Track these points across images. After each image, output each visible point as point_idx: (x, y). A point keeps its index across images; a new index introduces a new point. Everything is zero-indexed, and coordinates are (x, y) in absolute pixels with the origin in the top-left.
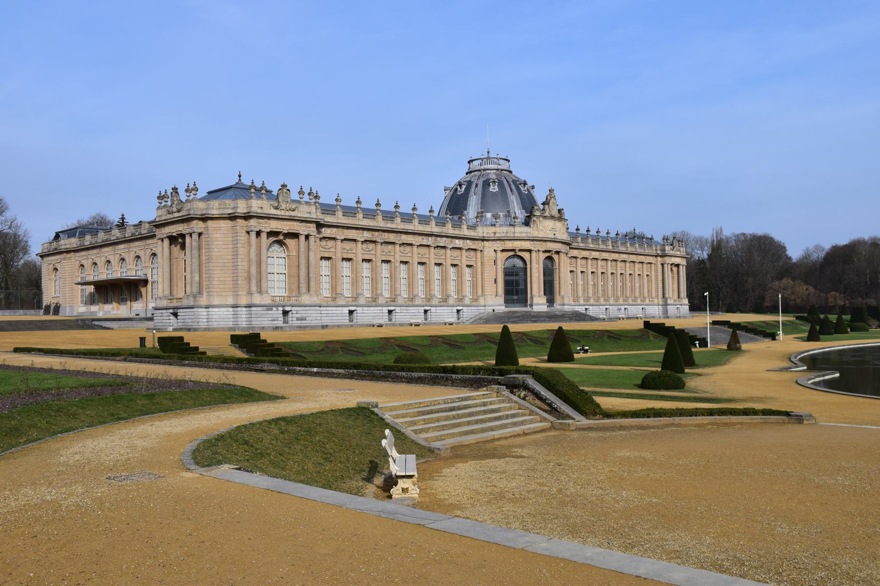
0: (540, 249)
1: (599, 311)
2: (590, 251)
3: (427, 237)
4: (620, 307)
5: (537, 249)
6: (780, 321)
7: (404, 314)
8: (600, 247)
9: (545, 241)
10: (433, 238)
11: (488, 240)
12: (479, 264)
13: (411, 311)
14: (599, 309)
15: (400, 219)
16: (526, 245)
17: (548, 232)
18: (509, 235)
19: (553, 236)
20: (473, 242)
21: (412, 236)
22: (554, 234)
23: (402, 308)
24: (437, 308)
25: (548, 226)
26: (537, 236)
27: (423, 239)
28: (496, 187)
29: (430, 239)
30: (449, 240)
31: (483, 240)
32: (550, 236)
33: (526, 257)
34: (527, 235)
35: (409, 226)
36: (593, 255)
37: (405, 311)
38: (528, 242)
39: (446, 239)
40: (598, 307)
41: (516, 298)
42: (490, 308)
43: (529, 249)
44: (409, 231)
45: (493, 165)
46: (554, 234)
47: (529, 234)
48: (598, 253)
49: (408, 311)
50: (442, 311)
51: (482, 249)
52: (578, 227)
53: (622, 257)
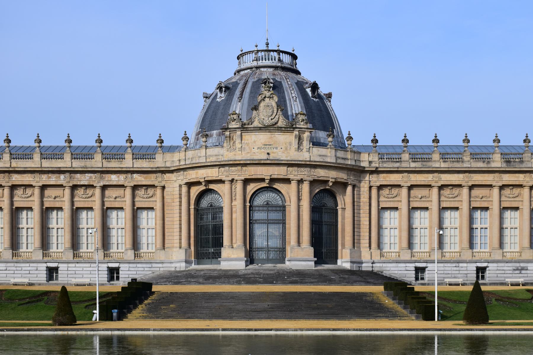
0: (236, 178)
1: (458, 272)
2: (436, 175)
3: (58, 175)
4: (522, 265)
5: (230, 179)
6: (434, 292)
7: (13, 272)
8: (411, 166)
9: (245, 165)
10: (67, 175)
11: (172, 172)
12: (158, 206)
13: (24, 269)
14: (455, 269)
15: (9, 155)
16: (213, 173)
17: (256, 150)
18: (194, 161)
19: (265, 157)
20: (145, 175)
21: (29, 175)
22: (268, 154)
23: (9, 264)
24: (70, 265)
25: (255, 142)
26: (232, 158)
27: (49, 178)
28: (223, 95)
29: (62, 176)
30: (98, 175)
31: (163, 172)
33: (197, 191)
34: (217, 159)
35: (25, 163)
37: (14, 269)
38: (216, 170)
39: (92, 175)
40: (454, 265)
41: (213, 251)
42: (173, 265)
43: (219, 178)
47: (220, 157)
48: (461, 176)
49: (18, 269)
50: (78, 269)
51: (162, 184)
52: (375, 137)
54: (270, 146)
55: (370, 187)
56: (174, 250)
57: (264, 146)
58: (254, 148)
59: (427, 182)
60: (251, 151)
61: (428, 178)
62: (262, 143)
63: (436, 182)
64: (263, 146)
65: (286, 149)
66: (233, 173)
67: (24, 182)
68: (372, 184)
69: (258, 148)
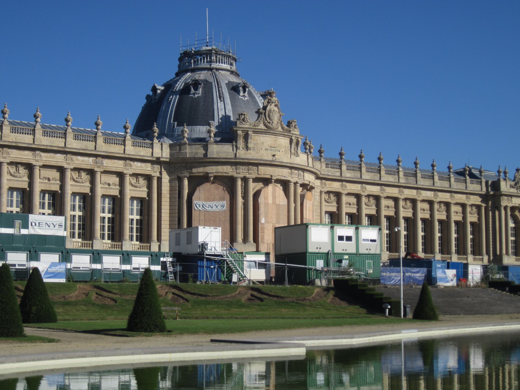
19: (270, 158)
22: (274, 156)
32: (265, 158)
36: (368, 190)
44: (20, 145)
45: (221, 64)
46: (274, 156)
53: (423, 195)
54: (275, 149)
55: (321, 192)
56: (127, 242)
57: (270, 148)
58: (262, 149)
59: (357, 191)
60: (260, 151)
61: (358, 187)
62: (268, 145)
63: (363, 192)
64: (270, 148)
65: (286, 152)
66: (243, 171)
67: (52, 162)
68: (322, 190)
69: (266, 149)
